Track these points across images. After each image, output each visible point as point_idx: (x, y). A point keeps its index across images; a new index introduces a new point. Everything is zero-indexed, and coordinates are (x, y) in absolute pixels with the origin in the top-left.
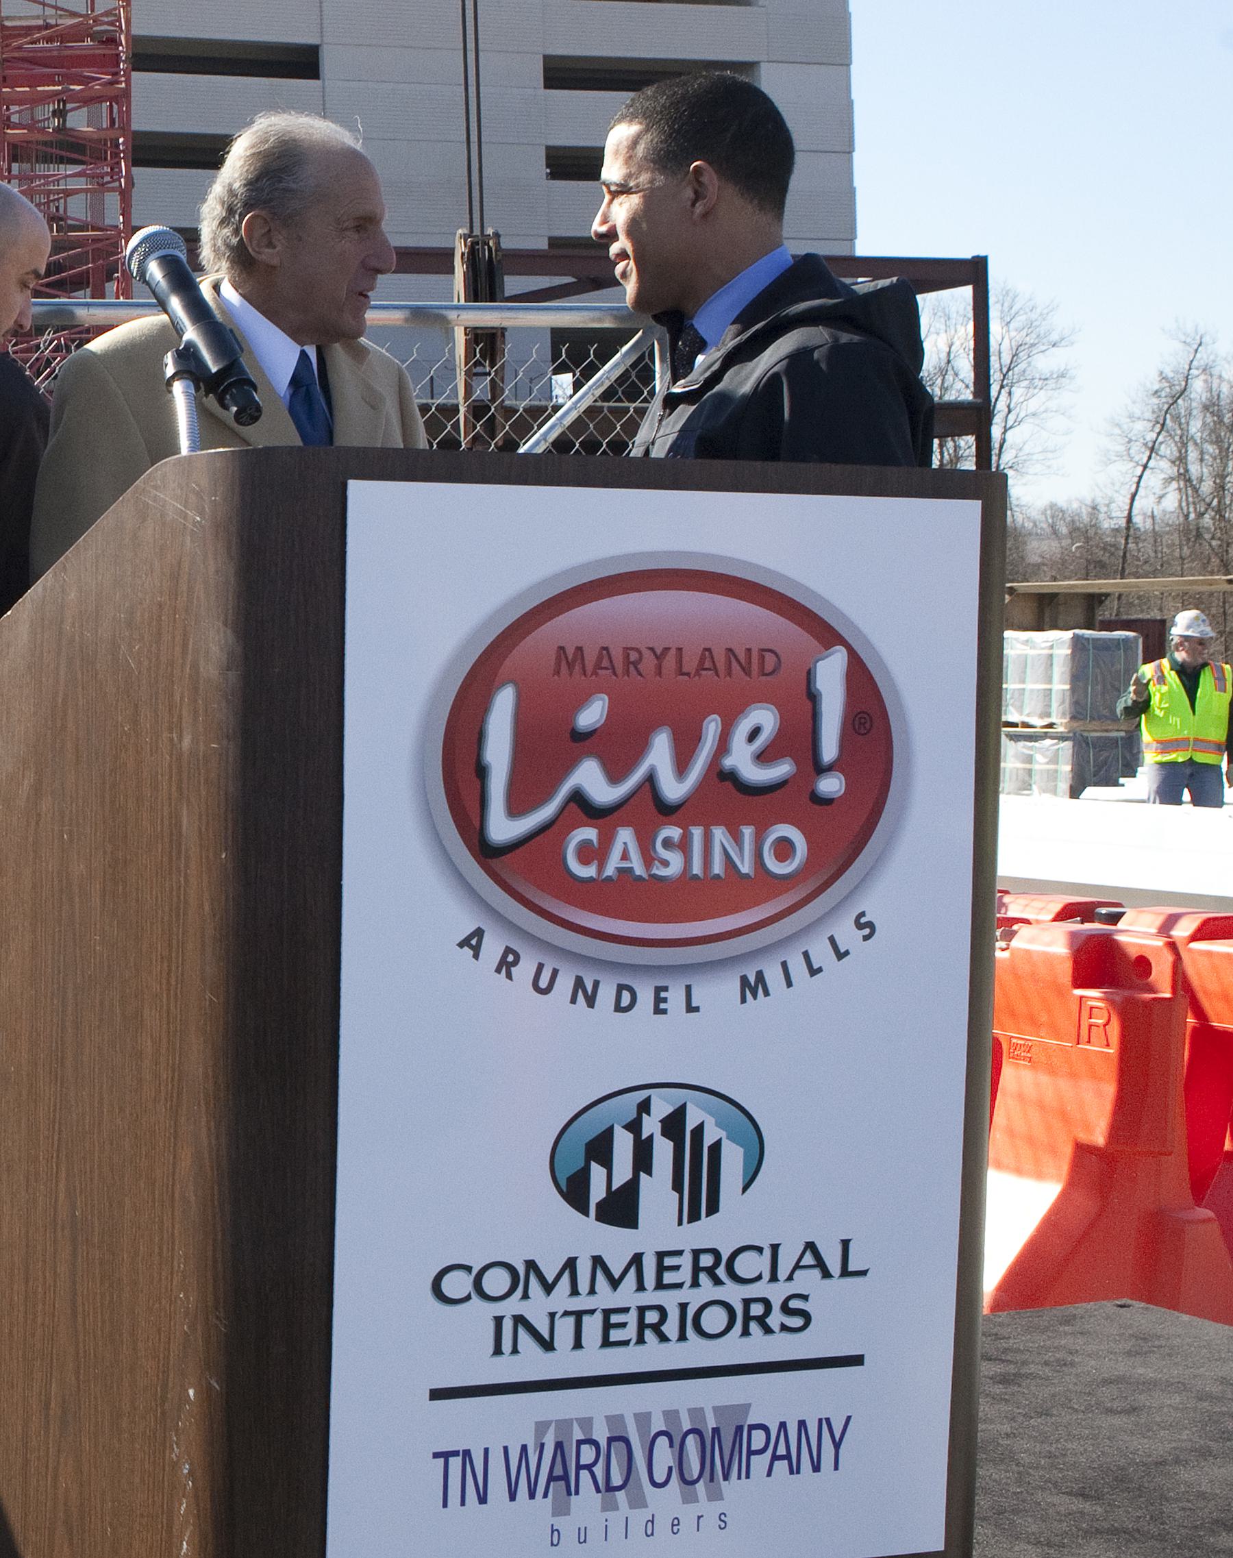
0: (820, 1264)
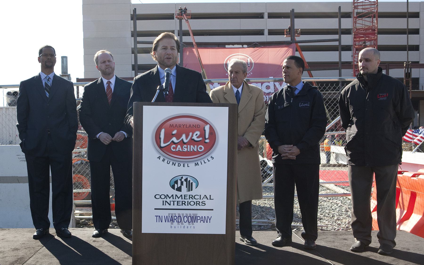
0: (207, 198)
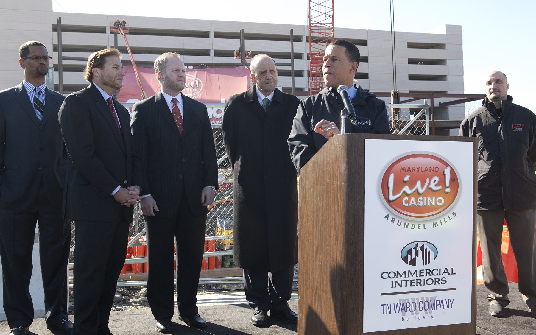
0: (448, 272)
